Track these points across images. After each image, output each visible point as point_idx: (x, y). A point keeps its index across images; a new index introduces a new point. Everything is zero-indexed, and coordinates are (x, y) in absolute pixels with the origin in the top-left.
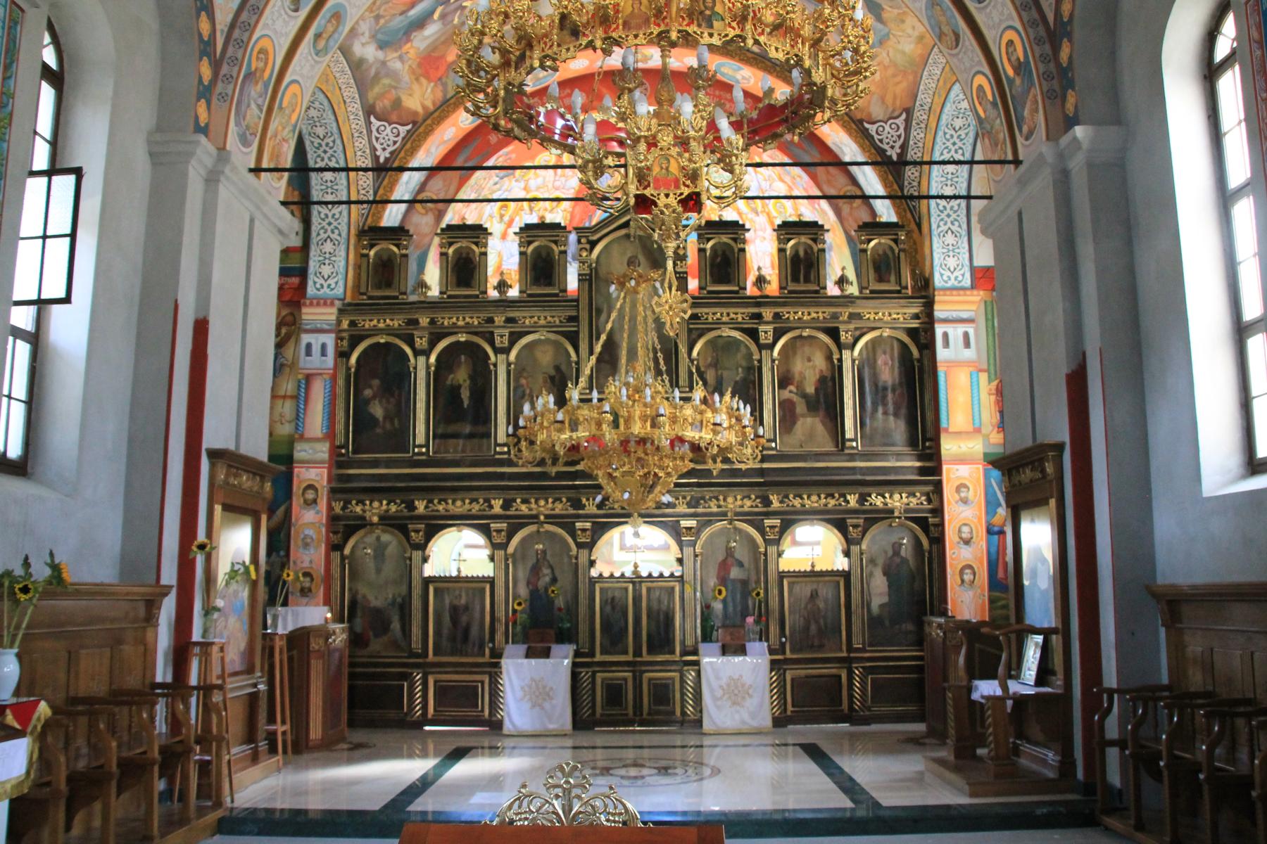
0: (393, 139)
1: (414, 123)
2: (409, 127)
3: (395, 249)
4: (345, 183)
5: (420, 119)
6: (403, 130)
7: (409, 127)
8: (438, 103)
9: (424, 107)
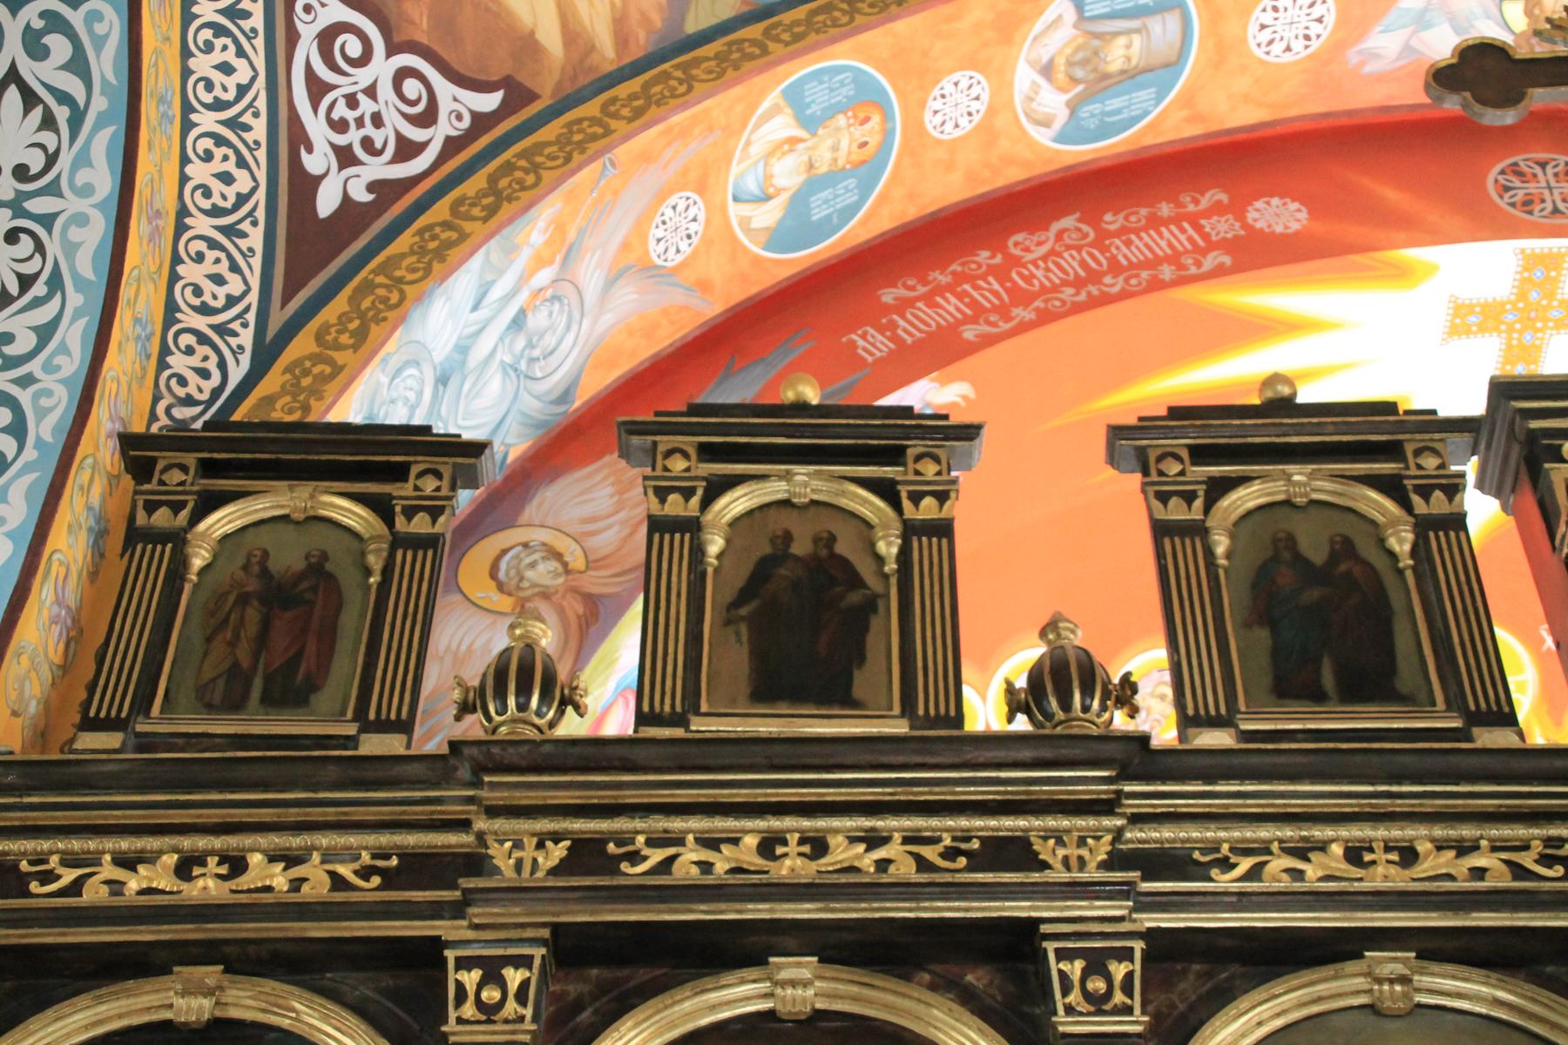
0: (395, 121)
1: (517, 96)
2: (489, 102)
3: (353, 515)
4: (104, 181)
5: (546, 90)
6: (459, 105)
7: (489, 102)
8: (642, 43)
9: (572, 34)
